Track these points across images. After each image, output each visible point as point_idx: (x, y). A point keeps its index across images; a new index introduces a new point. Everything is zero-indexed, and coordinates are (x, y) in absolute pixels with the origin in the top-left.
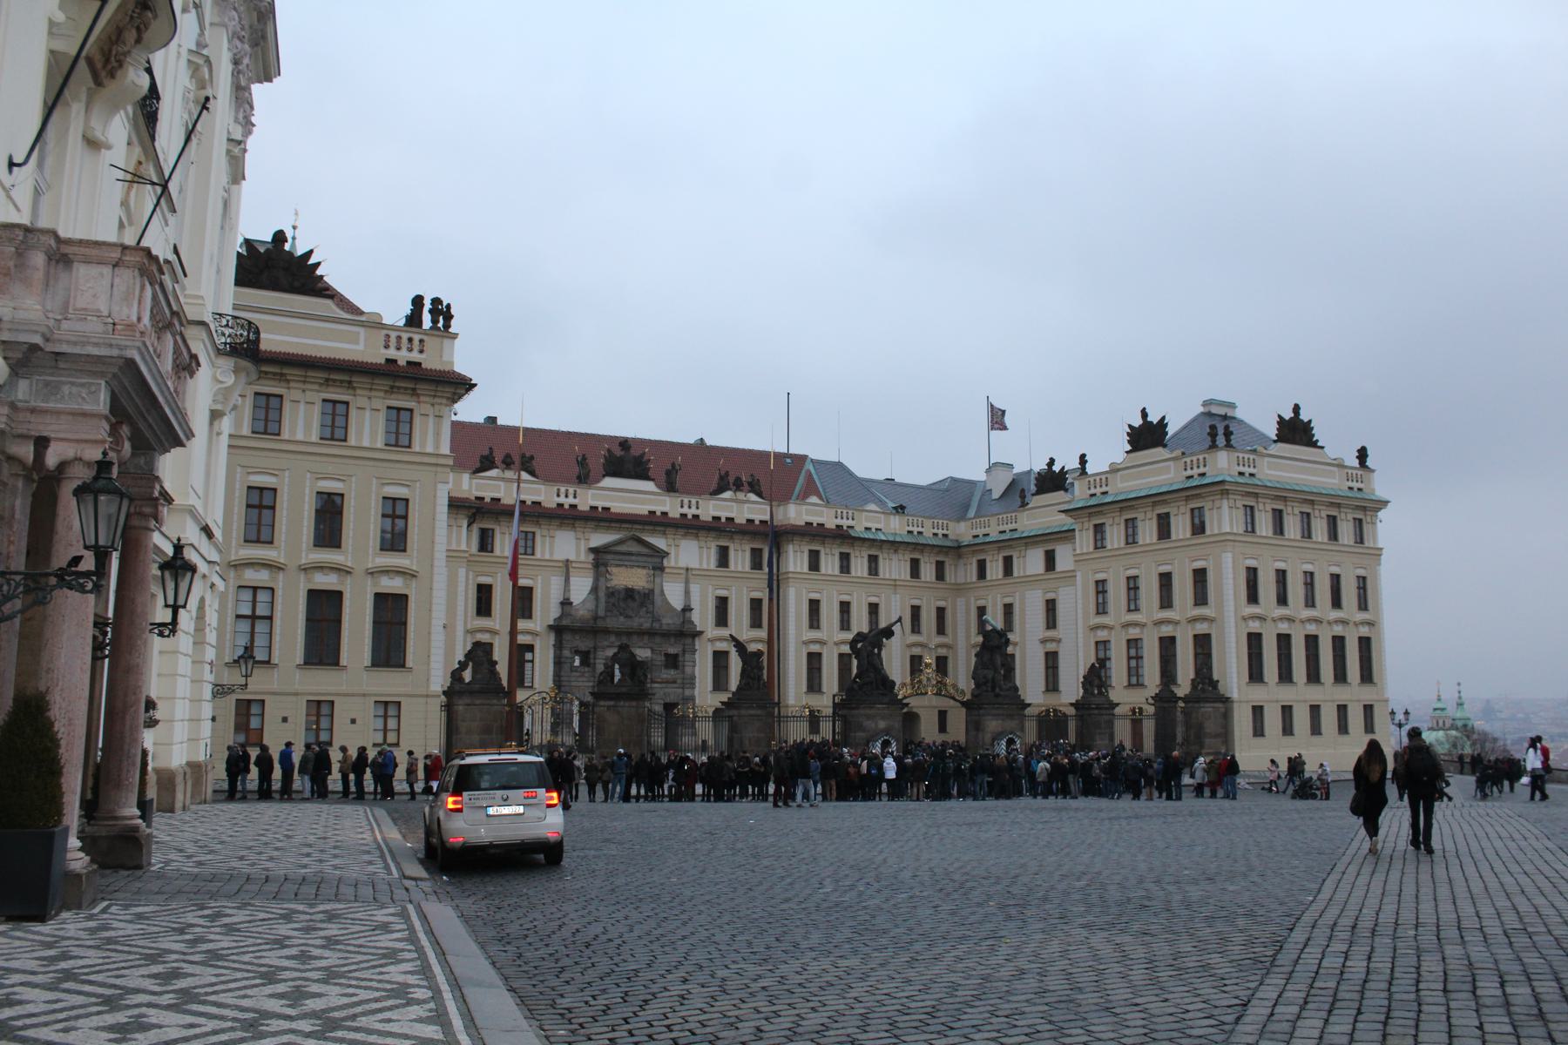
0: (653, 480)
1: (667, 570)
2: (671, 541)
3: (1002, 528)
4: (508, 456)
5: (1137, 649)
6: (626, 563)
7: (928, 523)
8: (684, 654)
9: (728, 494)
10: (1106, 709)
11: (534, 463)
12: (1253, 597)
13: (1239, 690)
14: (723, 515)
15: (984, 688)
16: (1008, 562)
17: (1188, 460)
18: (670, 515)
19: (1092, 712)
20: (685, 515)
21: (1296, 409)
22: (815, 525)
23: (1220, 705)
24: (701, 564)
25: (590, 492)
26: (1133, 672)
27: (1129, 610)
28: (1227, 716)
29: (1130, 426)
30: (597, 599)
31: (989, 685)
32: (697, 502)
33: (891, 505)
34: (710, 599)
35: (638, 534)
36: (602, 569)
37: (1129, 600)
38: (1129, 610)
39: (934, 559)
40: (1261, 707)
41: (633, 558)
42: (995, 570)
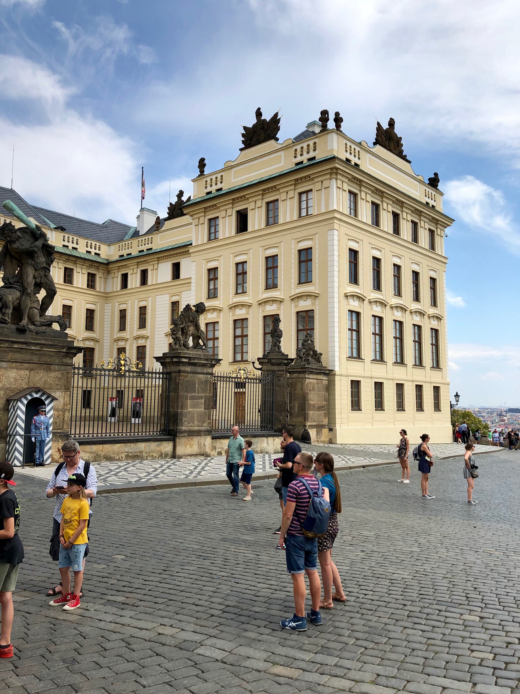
3: (141, 248)
5: (243, 328)
7: (82, 242)
10: (204, 365)
12: (354, 279)
13: (340, 363)
16: (144, 274)
17: (298, 147)
19: (182, 368)
21: (392, 123)
23: (325, 378)
26: (239, 349)
27: (237, 293)
28: (330, 388)
29: (245, 128)
31: (10, 311)
33: (53, 226)
37: (237, 284)
38: (237, 293)
39: (86, 272)
40: (358, 382)
42: (134, 280)
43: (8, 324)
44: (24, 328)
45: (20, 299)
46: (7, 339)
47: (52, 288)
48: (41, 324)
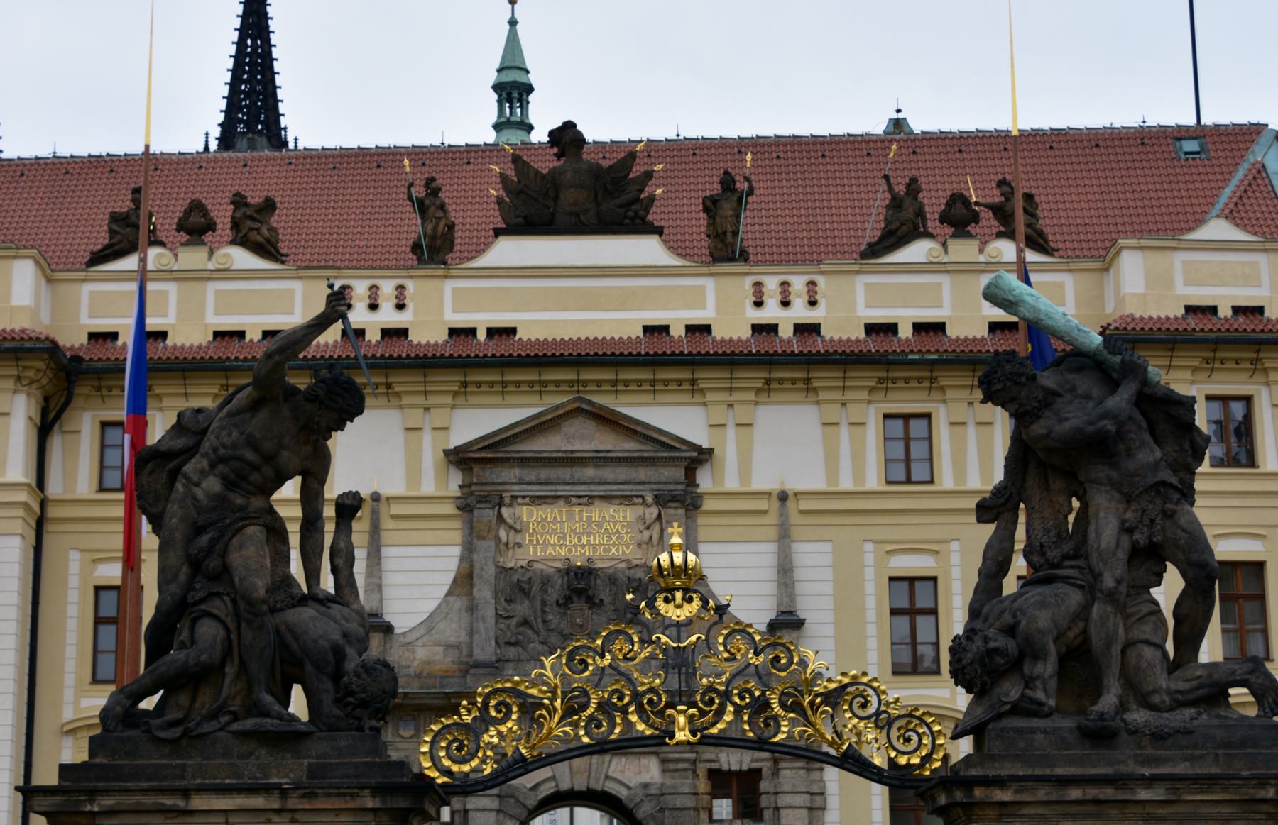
0: (659, 231)
1: (708, 505)
2: (720, 413)
4: (197, 207)
6: (562, 490)
8: (776, 772)
9: (918, 251)
11: (274, 221)
14: (905, 316)
15: (1011, 691)
18: (718, 333)
20: (772, 329)
22: (1225, 312)
24: (832, 470)
25: (449, 286)
30: (472, 608)
31: (1047, 668)
32: (812, 284)
34: (870, 588)
35: (600, 400)
36: (486, 514)
41: (590, 472)
43: (1047, 716)
44: (1099, 724)
45: (1083, 614)
46: (1048, 772)
47: (1194, 557)
48: (1176, 701)
